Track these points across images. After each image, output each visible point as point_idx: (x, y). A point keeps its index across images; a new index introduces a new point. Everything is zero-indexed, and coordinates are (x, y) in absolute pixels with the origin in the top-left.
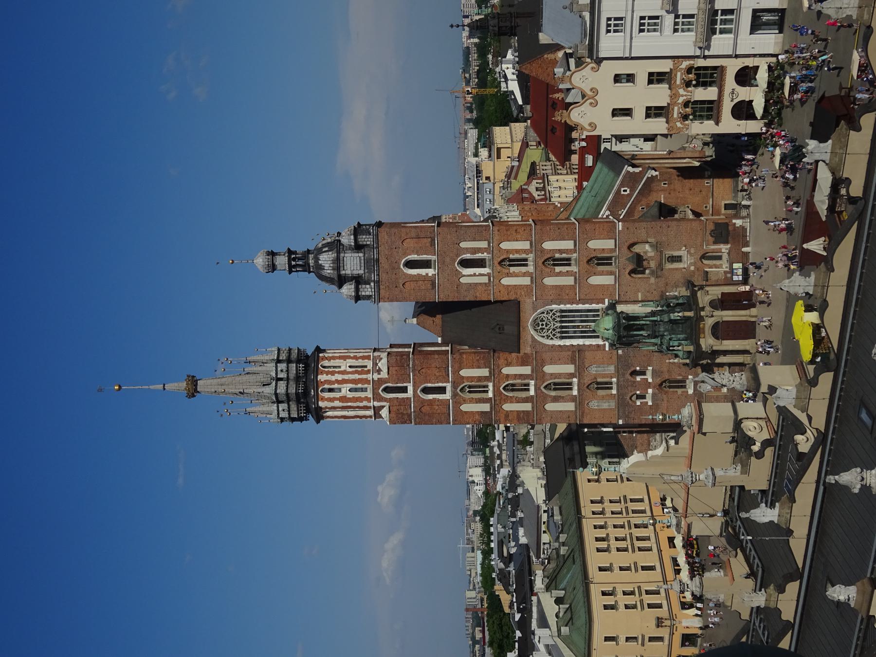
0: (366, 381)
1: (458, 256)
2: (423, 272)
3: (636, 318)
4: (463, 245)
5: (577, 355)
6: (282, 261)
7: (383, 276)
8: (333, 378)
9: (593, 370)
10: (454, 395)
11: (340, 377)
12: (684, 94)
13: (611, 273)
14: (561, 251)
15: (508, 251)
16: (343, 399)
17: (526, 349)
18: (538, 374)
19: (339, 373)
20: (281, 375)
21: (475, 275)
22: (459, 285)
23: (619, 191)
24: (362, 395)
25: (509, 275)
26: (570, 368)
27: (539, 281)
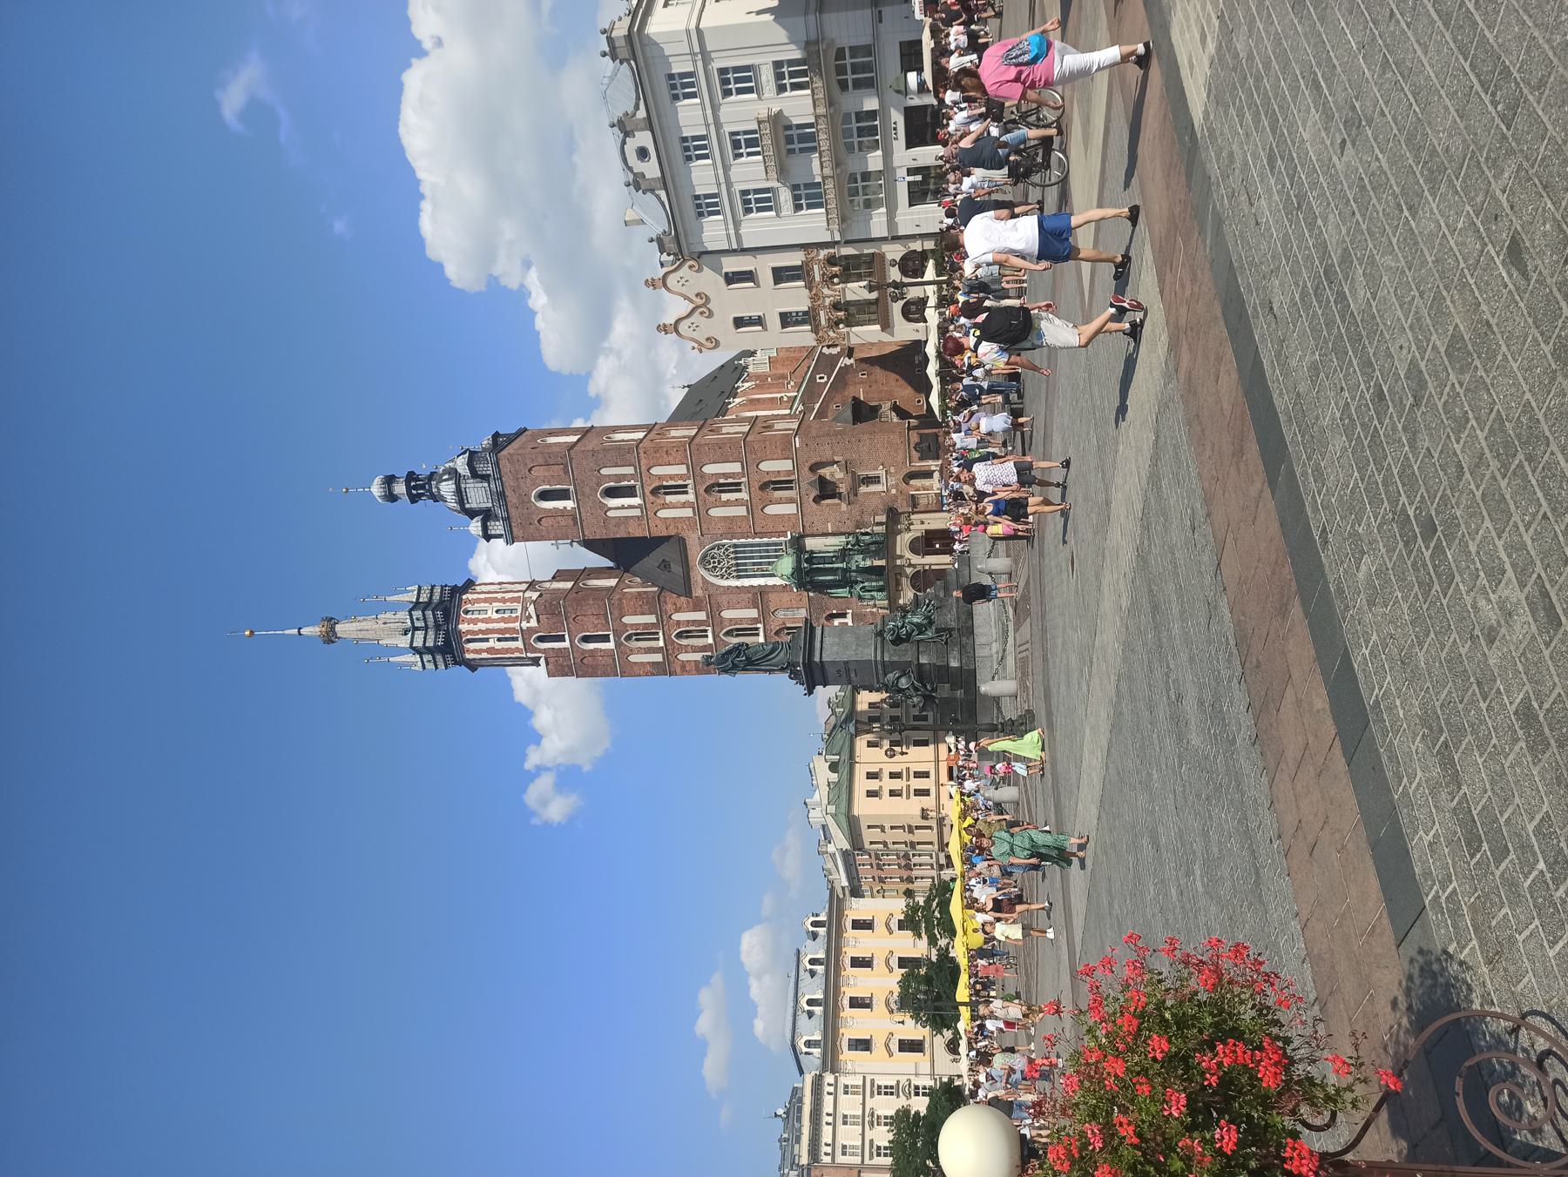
0: (514, 630)
1: (599, 485)
2: (560, 504)
3: (824, 560)
4: (604, 471)
5: (759, 597)
6: (400, 488)
7: (513, 512)
8: (476, 628)
9: (781, 614)
10: (618, 644)
11: (482, 626)
12: (829, 294)
13: (791, 501)
14: (725, 475)
15: (660, 477)
16: (488, 650)
17: (698, 592)
18: (714, 619)
19: (483, 621)
20: (417, 624)
21: (623, 507)
22: (607, 519)
23: (812, 378)
24: (512, 644)
25: (665, 506)
26: (753, 613)
27: (703, 512)
